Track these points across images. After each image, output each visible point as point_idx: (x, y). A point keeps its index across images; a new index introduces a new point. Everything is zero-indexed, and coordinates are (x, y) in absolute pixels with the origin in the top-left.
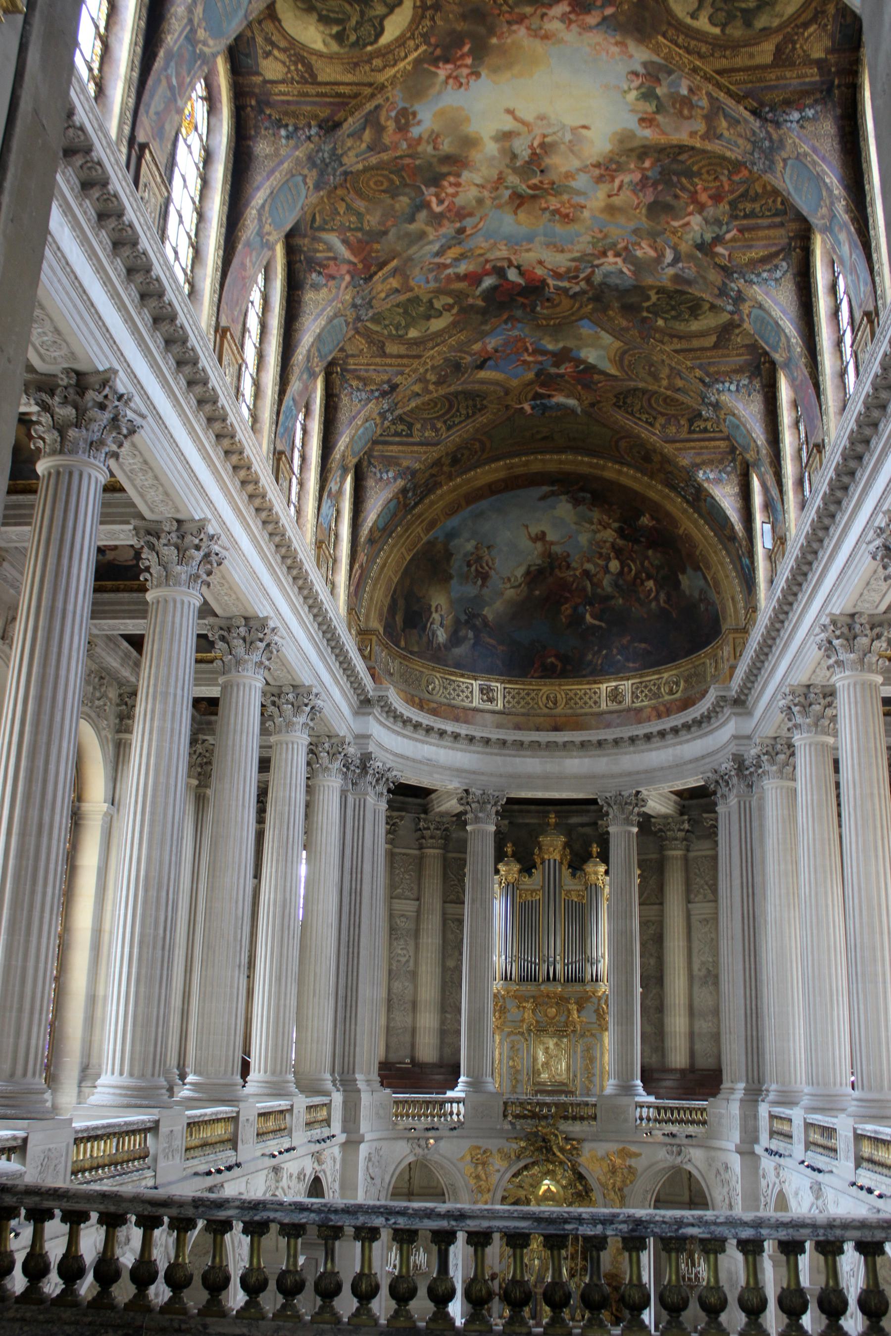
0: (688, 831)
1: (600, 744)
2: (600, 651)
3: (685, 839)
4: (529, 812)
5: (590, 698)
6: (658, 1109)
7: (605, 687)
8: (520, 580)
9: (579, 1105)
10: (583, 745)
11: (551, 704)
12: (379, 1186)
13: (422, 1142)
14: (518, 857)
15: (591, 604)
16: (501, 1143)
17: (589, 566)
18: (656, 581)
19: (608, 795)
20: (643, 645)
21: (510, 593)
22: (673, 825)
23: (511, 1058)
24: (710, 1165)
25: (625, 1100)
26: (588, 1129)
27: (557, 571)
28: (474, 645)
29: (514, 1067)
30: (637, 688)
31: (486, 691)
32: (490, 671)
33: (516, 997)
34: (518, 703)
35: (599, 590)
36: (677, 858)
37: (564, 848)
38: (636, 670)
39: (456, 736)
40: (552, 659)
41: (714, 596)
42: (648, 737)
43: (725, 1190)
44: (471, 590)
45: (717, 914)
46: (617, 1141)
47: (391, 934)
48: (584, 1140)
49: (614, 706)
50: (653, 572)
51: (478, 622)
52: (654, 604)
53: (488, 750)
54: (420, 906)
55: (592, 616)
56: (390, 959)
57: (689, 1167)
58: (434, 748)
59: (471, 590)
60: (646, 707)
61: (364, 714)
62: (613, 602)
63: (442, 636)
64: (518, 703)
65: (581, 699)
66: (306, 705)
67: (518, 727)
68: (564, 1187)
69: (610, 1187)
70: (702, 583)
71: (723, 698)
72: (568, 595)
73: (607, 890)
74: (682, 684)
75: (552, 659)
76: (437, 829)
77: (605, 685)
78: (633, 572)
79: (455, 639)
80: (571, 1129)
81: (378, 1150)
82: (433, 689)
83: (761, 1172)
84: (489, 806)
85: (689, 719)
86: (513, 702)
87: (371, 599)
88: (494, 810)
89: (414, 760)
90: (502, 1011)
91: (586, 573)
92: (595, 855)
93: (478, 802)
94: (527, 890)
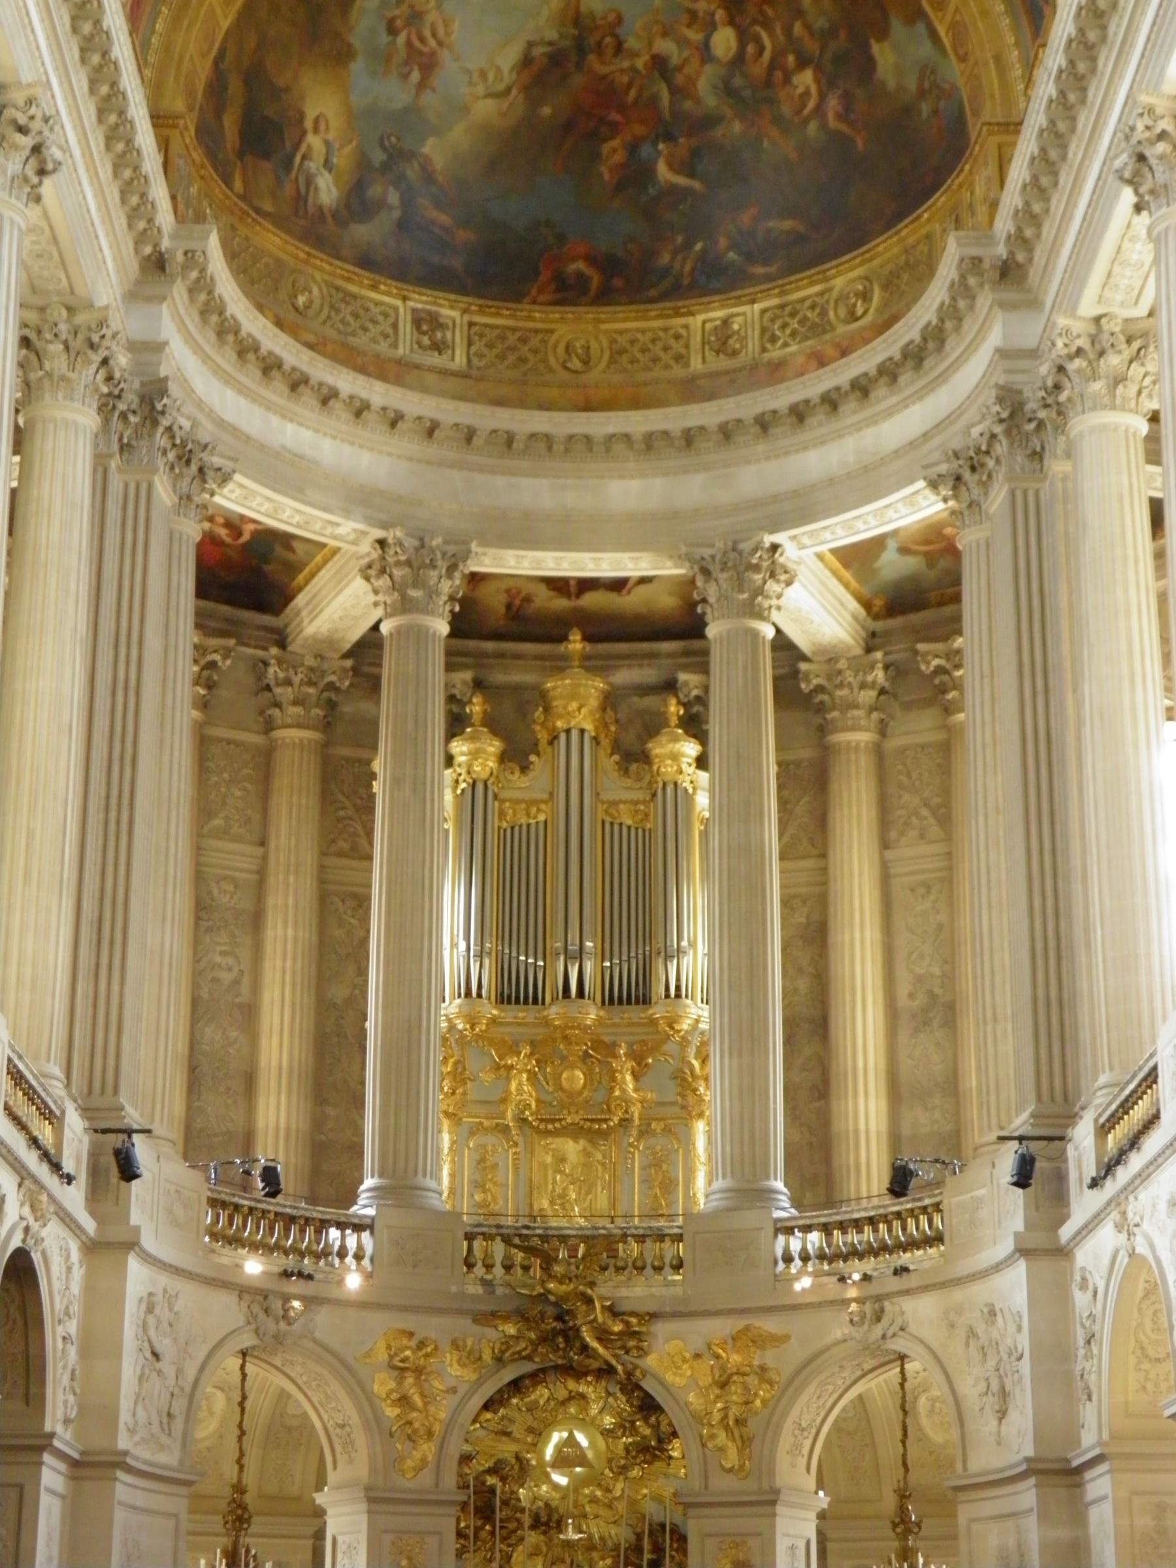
0: (882, 691)
1: (689, 438)
2: (688, 245)
3: (873, 709)
4: (518, 656)
5: (666, 349)
6: (826, 1229)
7: (704, 318)
8: (508, 78)
9: (641, 1239)
10: (651, 443)
11: (575, 364)
12: (171, 1381)
13: (277, 1305)
14: (493, 725)
15: (669, 137)
16: (463, 1325)
17: (666, 47)
18: (818, 69)
19: (707, 552)
20: (787, 224)
21: (485, 109)
22: (849, 676)
23: (479, 1185)
24: (952, 1326)
25: (749, 1218)
26: (664, 1291)
27: (592, 58)
28: (402, 225)
29: (484, 1204)
30: (773, 320)
31: (425, 322)
32: (438, 279)
33: (491, 1042)
34: (502, 357)
35: (688, 105)
36: (857, 748)
37: (603, 709)
38: (769, 278)
39: (360, 410)
40: (580, 265)
41: (954, 72)
42: (799, 414)
43: (991, 1363)
44: (395, 93)
45: (950, 868)
46: (731, 1312)
47: (198, 919)
48: (653, 1316)
49: (724, 363)
50: (812, 47)
51: (412, 172)
52: (812, 127)
53: (432, 450)
54: (265, 858)
55: (671, 166)
56: (197, 976)
57: (899, 1345)
58: (307, 435)
59: (395, 93)
60: (792, 354)
61: (149, 299)
62: (718, 132)
63: (327, 191)
64: (502, 357)
65: (644, 351)
66: (22, 130)
67: (500, 402)
68: (607, 1433)
69: (716, 1417)
70: (926, 50)
71: (977, 261)
72: (615, 116)
73: (702, 801)
74: (877, 295)
75: (580, 265)
76: (311, 683)
77: (700, 318)
78: (767, 55)
79: (358, 203)
80: (623, 1292)
81: (171, 1299)
82: (308, 306)
83: (1077, 1277)
84: (434, 574)
85: (895, 351)
86: (491, 355)
87: (167, 48)
88: (446, 587)
89: (262, 447)
90: (459, 1076)
91: (659, 63)
92: (674, 721)
93: (408, 563)
94: (517, 802)
